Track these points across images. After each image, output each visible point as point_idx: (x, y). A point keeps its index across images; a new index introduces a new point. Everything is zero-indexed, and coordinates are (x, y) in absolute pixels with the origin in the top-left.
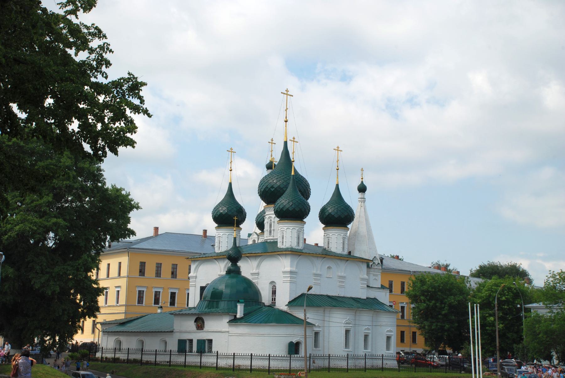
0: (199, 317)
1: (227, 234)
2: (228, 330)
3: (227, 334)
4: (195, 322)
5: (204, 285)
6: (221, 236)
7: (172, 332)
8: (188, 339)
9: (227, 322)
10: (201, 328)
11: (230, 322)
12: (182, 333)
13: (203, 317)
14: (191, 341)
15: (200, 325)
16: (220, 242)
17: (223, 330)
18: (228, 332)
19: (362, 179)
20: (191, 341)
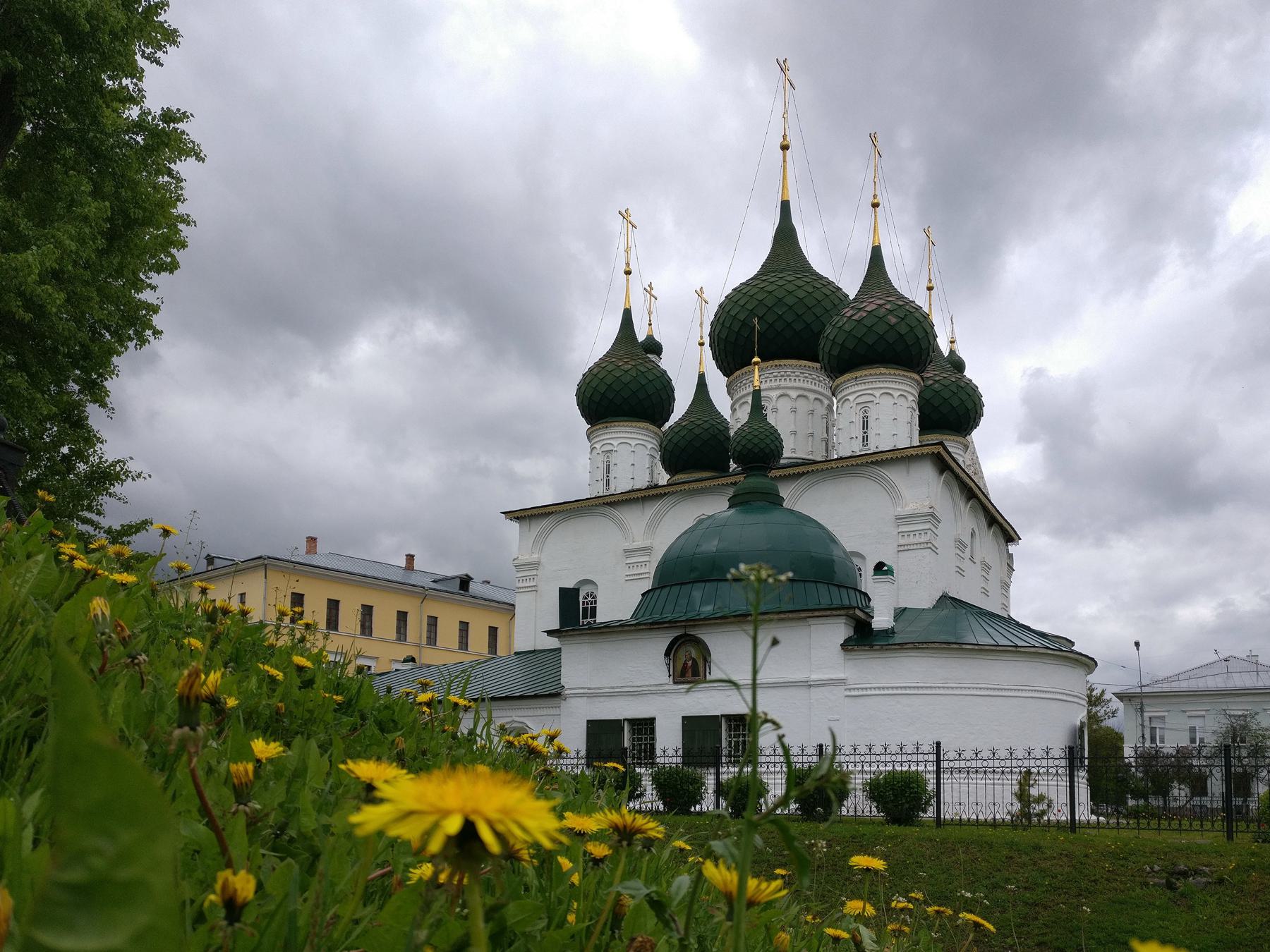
0: (686, 635)
1: (633, 443)
2: (842, 676)
3: (840, 692)
4: (667, 654)
5: (570, 584)
6: (615, 449)
7: (558, 695)
8: (629, 717)
9: (841, 645)
10: (696, 673)
11: (847, 646)
12: (602, 699)
13: (702, 637)
14: (645, 727)
15: (690, 663)
16: (608, 467)
17: (814, 677)
18: (841, 682)
19: (952, 342)
20: (645, 727)
